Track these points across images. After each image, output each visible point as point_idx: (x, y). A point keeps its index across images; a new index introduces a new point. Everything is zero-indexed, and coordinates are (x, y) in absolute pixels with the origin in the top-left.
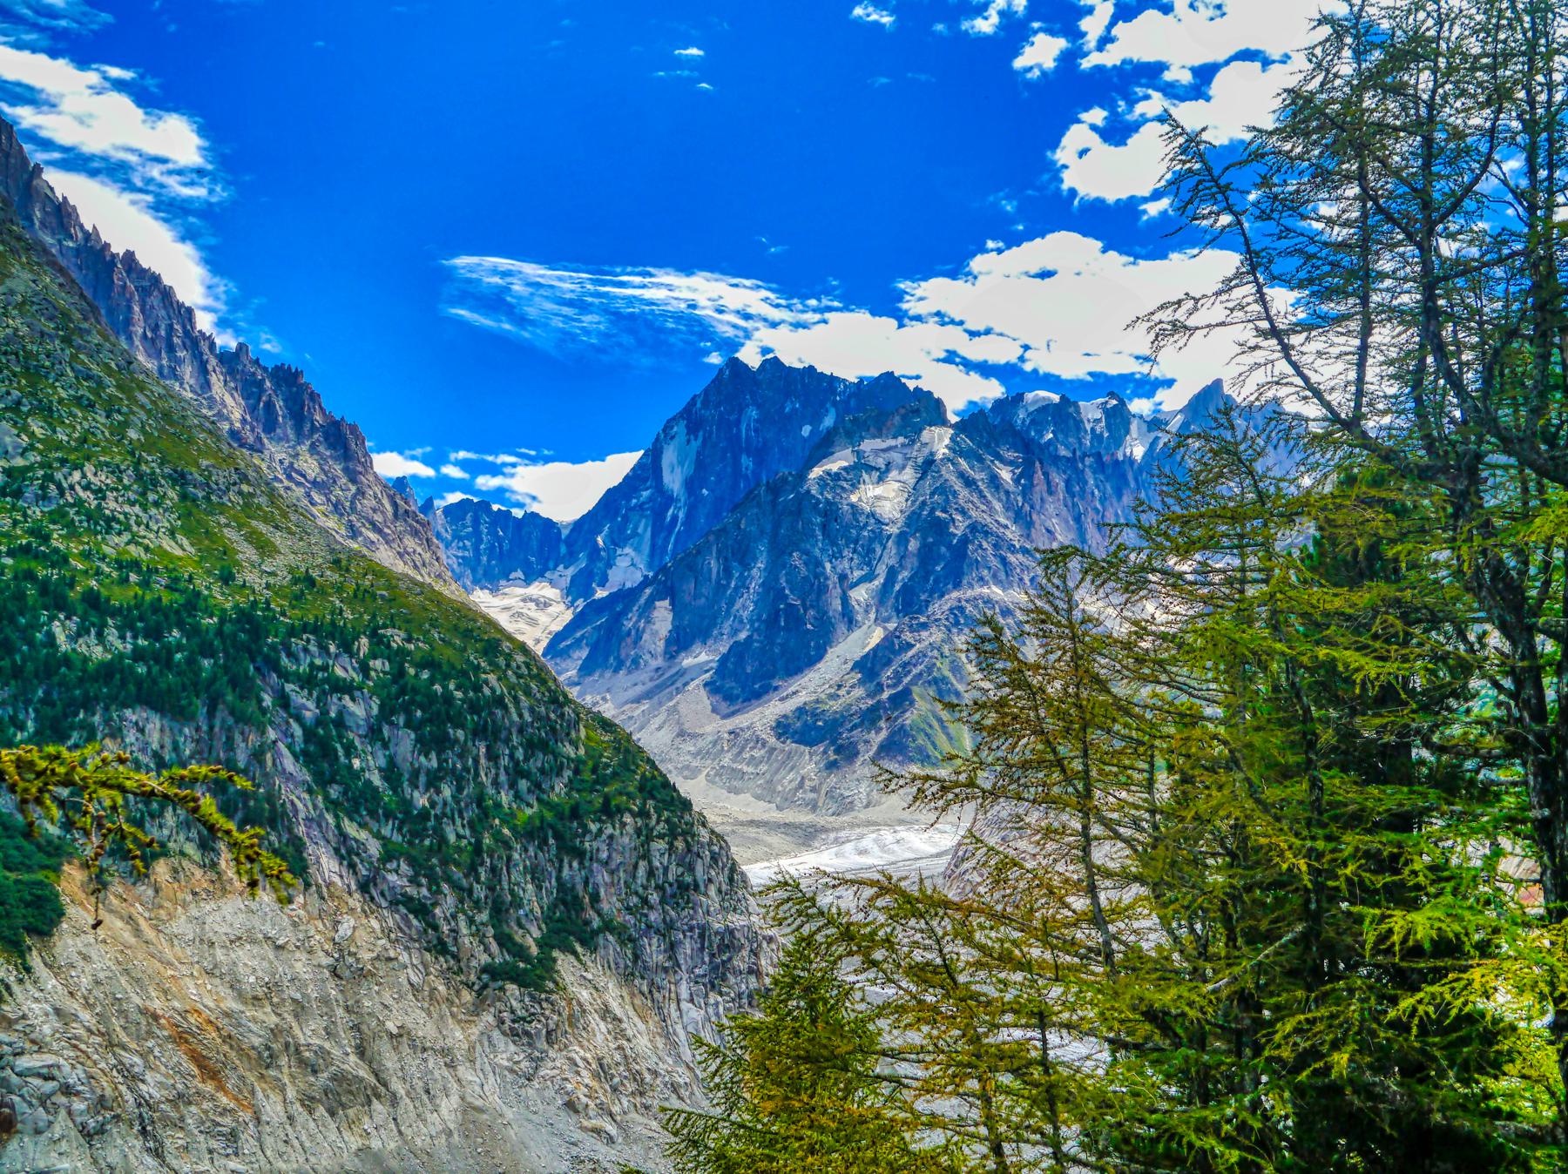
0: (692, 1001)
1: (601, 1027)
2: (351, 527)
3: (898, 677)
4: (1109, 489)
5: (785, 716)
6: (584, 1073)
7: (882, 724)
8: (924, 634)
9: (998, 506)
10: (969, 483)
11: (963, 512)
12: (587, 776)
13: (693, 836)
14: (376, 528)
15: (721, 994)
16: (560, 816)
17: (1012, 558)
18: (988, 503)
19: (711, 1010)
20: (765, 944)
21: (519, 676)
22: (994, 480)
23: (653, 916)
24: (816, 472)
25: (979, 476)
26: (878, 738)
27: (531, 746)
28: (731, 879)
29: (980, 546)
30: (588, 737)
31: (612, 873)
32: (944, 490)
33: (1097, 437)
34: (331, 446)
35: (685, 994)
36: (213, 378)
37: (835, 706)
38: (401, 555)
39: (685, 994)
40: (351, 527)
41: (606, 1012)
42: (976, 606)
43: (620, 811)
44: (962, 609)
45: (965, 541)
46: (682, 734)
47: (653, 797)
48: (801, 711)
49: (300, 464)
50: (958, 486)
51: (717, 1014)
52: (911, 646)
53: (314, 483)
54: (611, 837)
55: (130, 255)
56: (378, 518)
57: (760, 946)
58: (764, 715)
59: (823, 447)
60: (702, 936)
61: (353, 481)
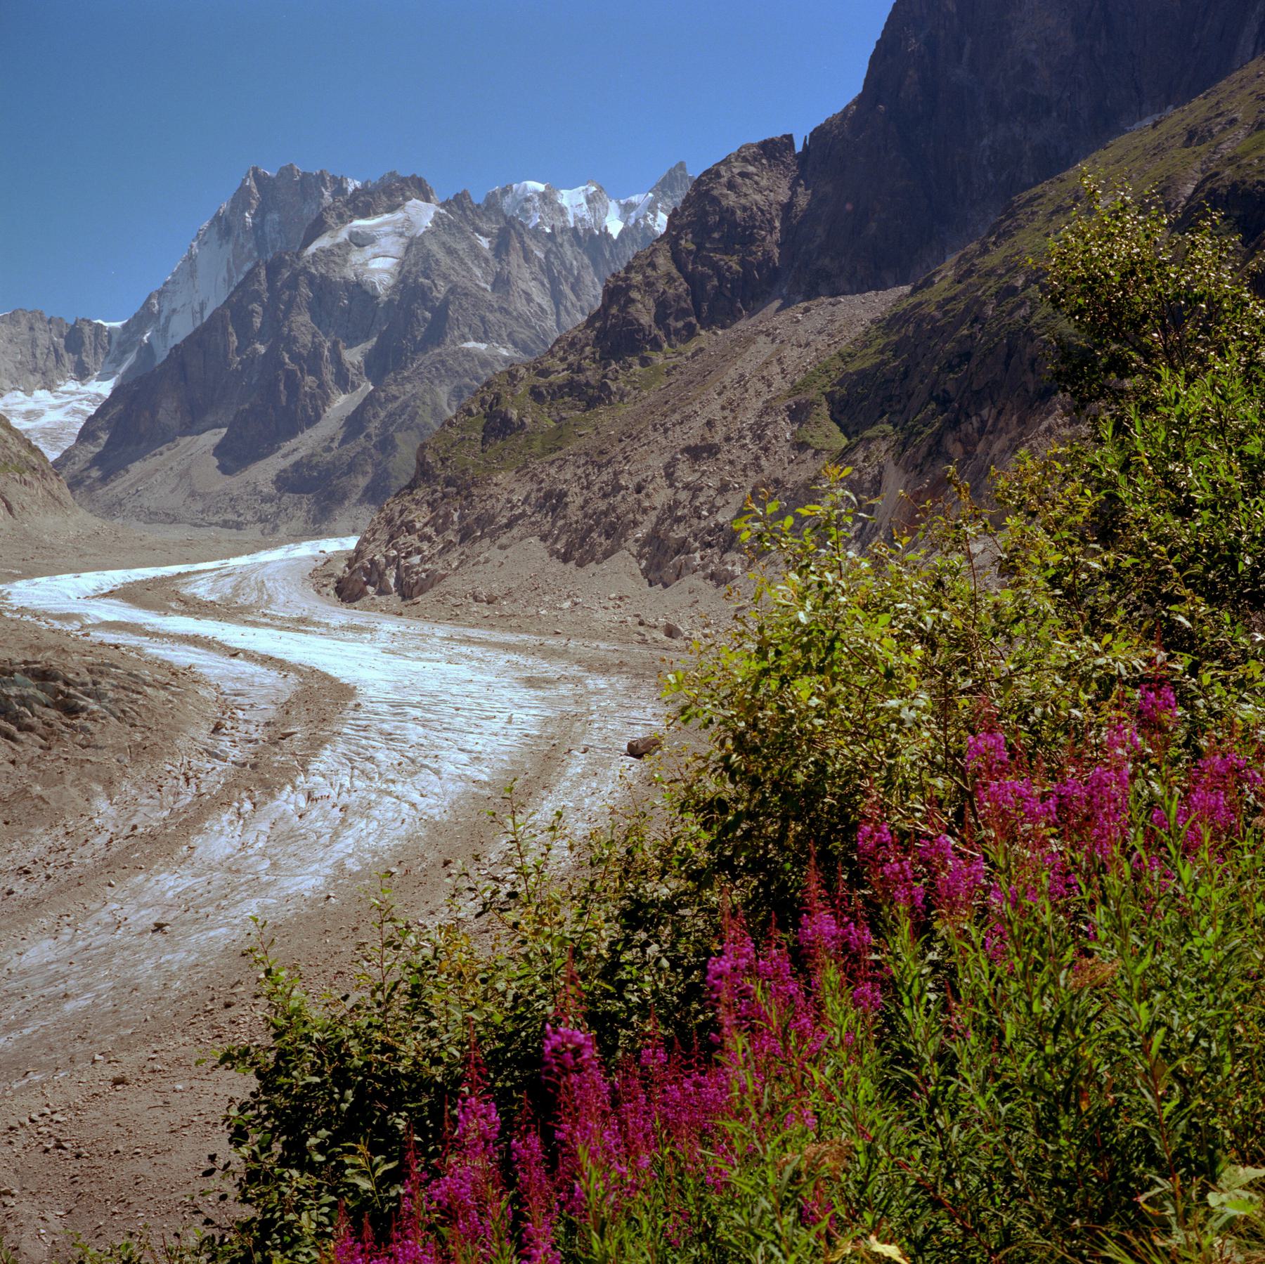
3: (385, 425)
4: (586, 260)
5: (284, 471)
8: (408, 387)
9: (478, 272)
10: (450, 252)
11: (445, 277)
17: (490, 317)
18: (469, 270)
22: (474, 248)
24: (312, 249)
25: (461, 246)
26: (363, 482)
29: (461, 306)
32: (428, 256)
37: (328, 457)
42: (455, 360)
44: (443, 362)
45: (446, 303)
46: (193, 494)
48: (297, 465)
50: (441, 255)
52: (396, 398)
58: (264, 472)
59: (318, 228)
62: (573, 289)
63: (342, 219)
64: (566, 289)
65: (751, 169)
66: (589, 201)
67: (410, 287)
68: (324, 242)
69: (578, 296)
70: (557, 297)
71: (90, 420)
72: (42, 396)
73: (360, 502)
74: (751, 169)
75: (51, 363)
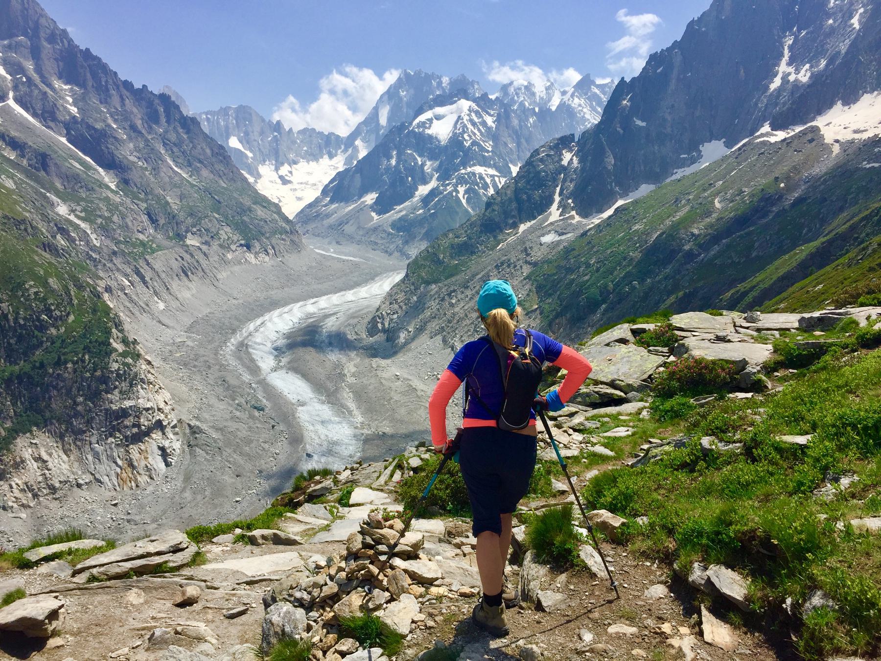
0: (98, 443)
1: (33, 465)
2: (189, 161)
6: (15, 490)
7: (426, 225)
12: (58, 344)
13: (107, 369)
14: (200, 162)
15: (115, 438)
16: (34, 368)
19: (107, 447)
20: (144, 412)
21: (26, 300)
23: (79, 408)
26: (424, 231)
27: (20, 339)
28: (131, 385)
30: (73, 321)
31: (58, 391)
33: (542, 98)
34: (182, 128)
35: (94, 439)
36: (127, 101)
38: (212, 172)
39: (94, 439)
40: (189, 161)
41: (38, 459)
43: (66, 362)
47: (89, 352)
49: (169, 136)
51: (111, 448)
53: (175, 144)
54: (58, 375)
55: (87, 50)
56: (202, 157)
57: (141, 413)
60: (106, 414)
61: (192, 142)
62: (526, 141)
63: (431, 108)
64: (523, 140)
65: (552, 153)
66: (547, 89)
67: (456, 141)
68: (422, 118)
69: (528, 144)
70: (519, 145)
71: (327, 186)
72: (313, 164)
73: (421, 240)
74: (552, 153)
75: (317, 152)
